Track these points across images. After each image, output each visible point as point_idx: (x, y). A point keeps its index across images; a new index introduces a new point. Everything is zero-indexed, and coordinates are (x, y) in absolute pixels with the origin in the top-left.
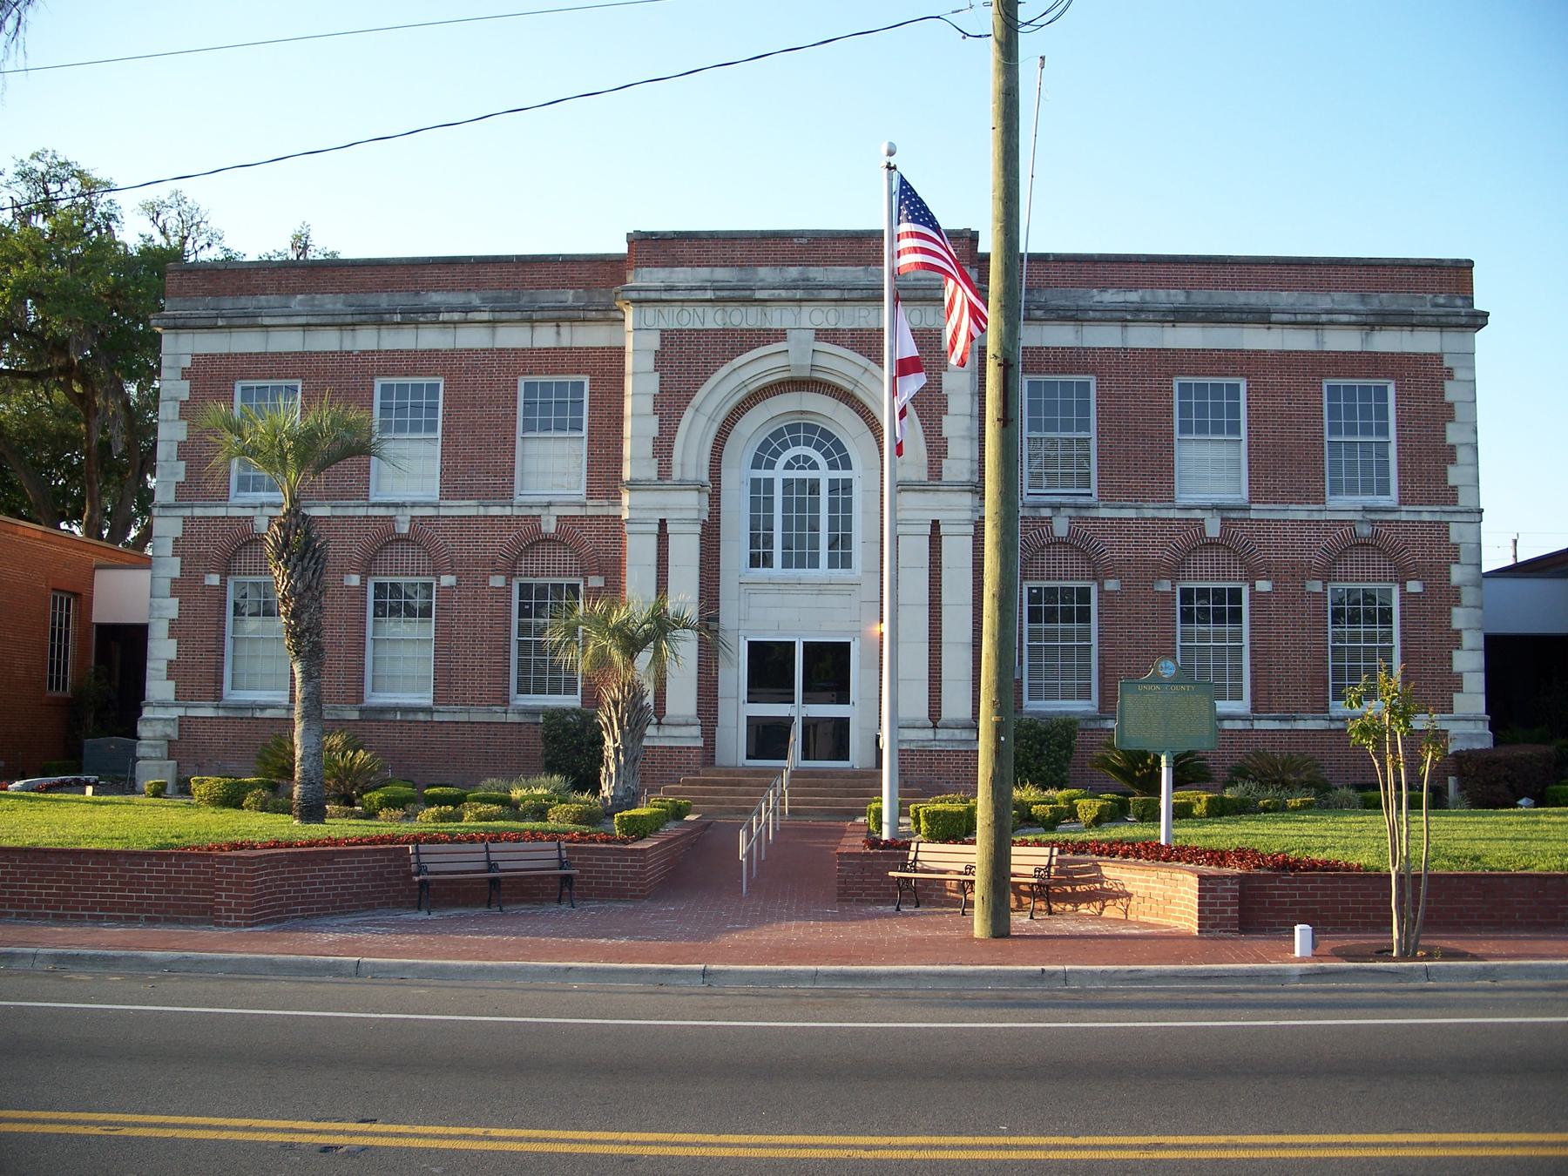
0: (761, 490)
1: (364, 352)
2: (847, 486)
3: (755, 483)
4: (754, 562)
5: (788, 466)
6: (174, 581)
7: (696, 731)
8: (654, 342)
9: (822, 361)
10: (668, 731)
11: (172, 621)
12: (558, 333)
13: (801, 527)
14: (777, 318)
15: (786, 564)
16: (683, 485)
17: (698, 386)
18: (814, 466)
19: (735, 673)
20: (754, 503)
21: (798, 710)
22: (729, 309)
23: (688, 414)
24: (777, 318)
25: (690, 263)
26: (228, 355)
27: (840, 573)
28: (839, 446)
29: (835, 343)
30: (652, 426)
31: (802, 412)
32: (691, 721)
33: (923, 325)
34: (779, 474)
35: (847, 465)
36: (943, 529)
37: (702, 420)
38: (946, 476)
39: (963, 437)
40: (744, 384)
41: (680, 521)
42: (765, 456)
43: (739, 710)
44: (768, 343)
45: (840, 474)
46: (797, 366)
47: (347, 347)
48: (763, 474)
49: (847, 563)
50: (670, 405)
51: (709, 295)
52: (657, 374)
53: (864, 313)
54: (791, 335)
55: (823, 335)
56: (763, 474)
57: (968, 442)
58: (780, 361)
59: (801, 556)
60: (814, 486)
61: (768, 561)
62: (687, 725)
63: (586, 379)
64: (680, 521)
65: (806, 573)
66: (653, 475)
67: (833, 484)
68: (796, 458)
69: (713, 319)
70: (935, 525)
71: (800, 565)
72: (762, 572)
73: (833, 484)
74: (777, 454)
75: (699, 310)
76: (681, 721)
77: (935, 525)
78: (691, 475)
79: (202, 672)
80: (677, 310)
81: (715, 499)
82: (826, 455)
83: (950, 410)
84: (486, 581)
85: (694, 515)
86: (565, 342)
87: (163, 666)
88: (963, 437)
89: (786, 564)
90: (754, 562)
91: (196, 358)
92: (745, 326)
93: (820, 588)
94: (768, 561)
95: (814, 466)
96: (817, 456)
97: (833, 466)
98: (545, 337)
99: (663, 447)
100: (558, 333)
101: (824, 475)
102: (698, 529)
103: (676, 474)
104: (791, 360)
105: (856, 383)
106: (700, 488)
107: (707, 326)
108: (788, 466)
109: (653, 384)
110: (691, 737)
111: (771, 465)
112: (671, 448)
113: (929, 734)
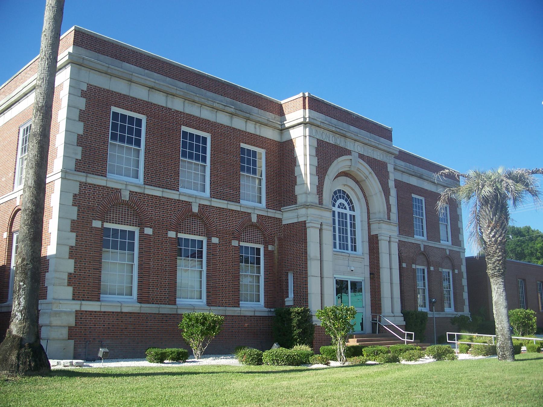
1: (177, 111)
6: (73, 221)
11: (71, 247)
18: (345, 208)
24: (349, 145)
26: (108, 91)
45: (352, 213)
47: (170, 106)
54: (353, 153)
55: (361, 156)
79: (86, 283)
84: (230, 243)
87: (66, 277)
91: (89, 86)
95: (345, 208)
96: (346, 204)
97: (350, 210)
98: (251, 128)
100: (255, 128)
101: (348, 212)
105: (367, 177)
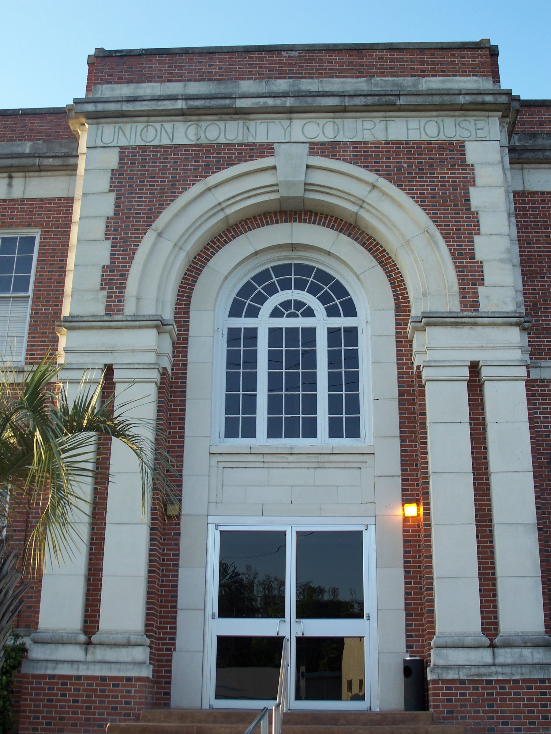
0: (240, 345)
2: (352, 334)
3: (233, 336)
4: (231, 430)
5: (276, 313)
7: (141, 654)
8: (112, 159)
9: (317, 178)
10: (100, 654)
12: (10, 185)
13: (292, 386)
14: (261, 131)
15: (274, 431)
16: (138, 322)
17: (162, 207)
18: (309, 313)
19: (202, 578)
20: (232, 360)
21: (290, 627)
22: (204, 124)
23: (149, 238)
25: (160, 79)
27: (345, 443)
28: (340, 290)
29: (334, 157)
30: (103, 253)
31: (293, 247)
32: (133, 639)
33: (442, 137)
34: (263, 323)
35: (350, 310)
36: (485, 373)
37: (166, 246)
38: (484, 306)
39: (502, 260)
40: (220, 207)
41: (130, 366)
42: (246, 302)
43: (203, 627)
44: (252, 158)
46: (287, 184)
48: (243, 322)
49: (354, 430)
50: (126, 231)
51: (180, 105)
52: (113, 196)
53: (368, 125)
55: (316, 148)
56: (243, 322)
57: (509, 266)
58: (267, 179)
59: (291, 419)
60: (310, 333)
61: (250, 431)
62: (128, 644)
63: (37, 234)
64: (130, 366)
65: (301, 443)
66: (99, 309)
67: (333, 333)
68: (286, 304)
69: (183, 134)
70: (474, 368)
71: (292, 433)
72: (240, 443)
73: (333, 333)
74: (262, 300)
75: (168, 126)
76: (121, 639)
77: (474, 368)
78: (149, 309)
80: (140, 126)
81: (181, 347)
82: (324, 299)
83: (484, 228)
85: (151, 358)
86: (17, 192)
88: (502, 260)
89: (274, 431)
90: (231, 430)
92: (222, 140)
93: (319, 460)
94: (250, 431)
95: (309, 313)
96: (312, 301)
97: (332, 312)
99: (114, 279)
100: (10, 185)
101: (322, 322)
102: (155, 375)
103: (130, 308)
104: (280, 176)
105: (361, 203)
106: (160, 325)
107: (176, 142)
108: (276, 313)
109: (107, 205)
110: (135, 662)
111: (253, 313)
112: (124, 277)
113: (486, 656)
